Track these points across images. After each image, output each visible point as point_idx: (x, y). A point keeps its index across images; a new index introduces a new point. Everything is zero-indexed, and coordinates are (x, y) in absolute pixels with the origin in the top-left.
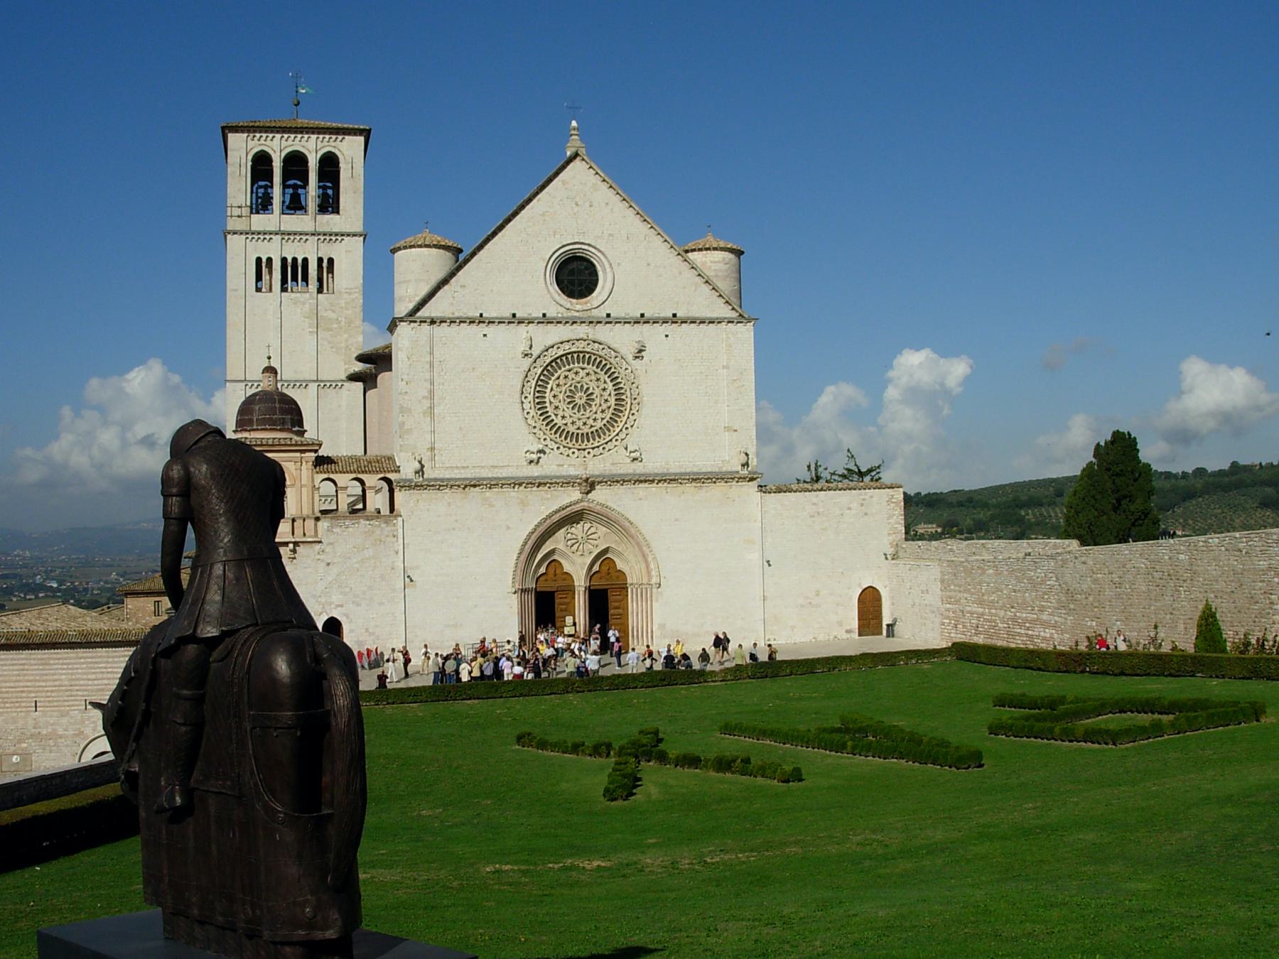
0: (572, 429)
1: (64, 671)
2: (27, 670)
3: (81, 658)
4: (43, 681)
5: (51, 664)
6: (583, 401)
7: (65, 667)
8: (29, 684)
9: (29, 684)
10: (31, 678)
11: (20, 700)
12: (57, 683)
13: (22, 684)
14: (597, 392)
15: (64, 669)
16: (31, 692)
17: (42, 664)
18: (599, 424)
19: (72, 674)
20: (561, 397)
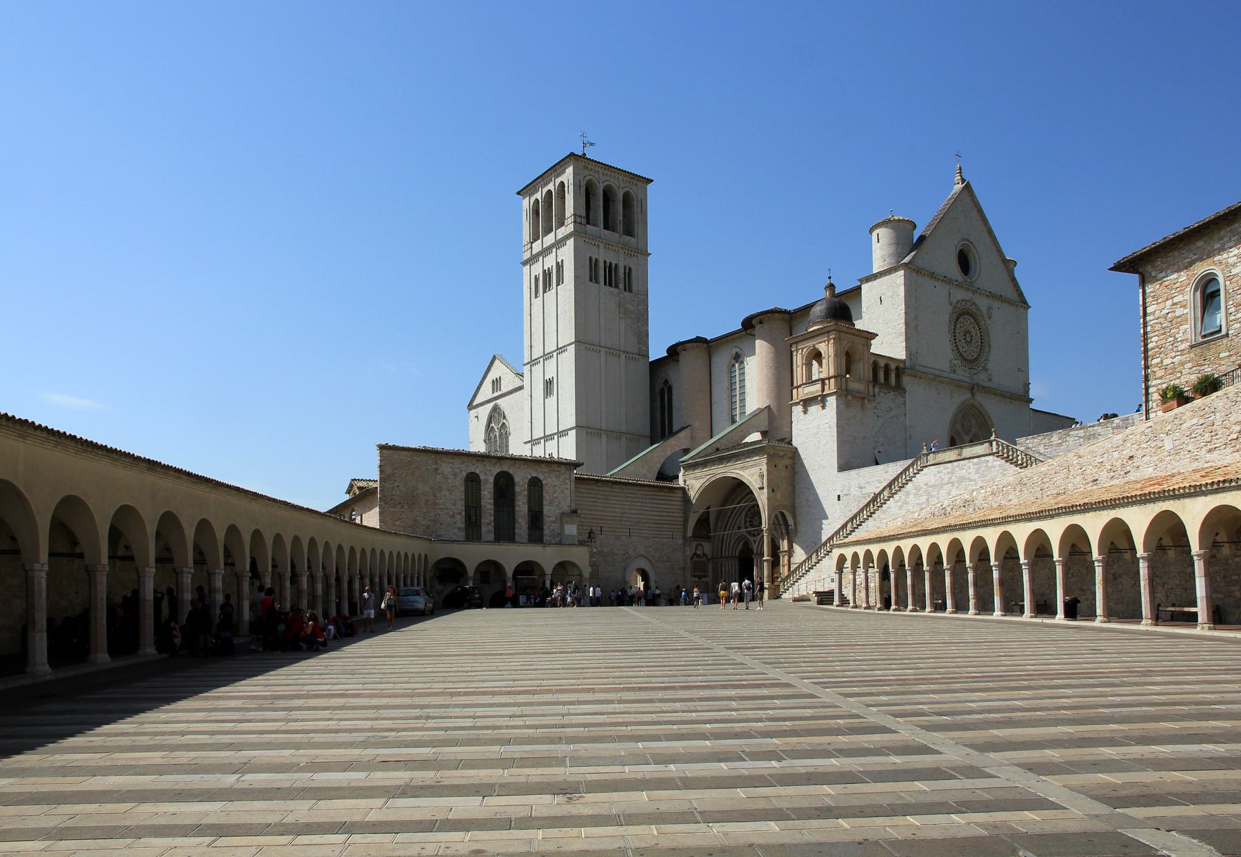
0: (965, 355)
1: (617, 506)
2: (596, 502)
3: (627, 497)
4: (606, 512)
5: (611, 500)
6: (969, 340)
7: (618, 502)
8: (597, 513)
9: (597, 513)
10: (599, 508)
11: (592, 524)
12: (613, 514)
13: (593, 513)
14: (974, 335)
15: (617, 504)
16: (598, 519)
17: (605, 499)
18: (975, 355)
19: (622, 508)
20: (962, 334)
